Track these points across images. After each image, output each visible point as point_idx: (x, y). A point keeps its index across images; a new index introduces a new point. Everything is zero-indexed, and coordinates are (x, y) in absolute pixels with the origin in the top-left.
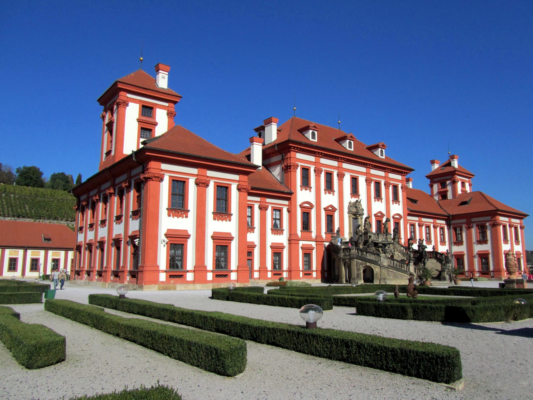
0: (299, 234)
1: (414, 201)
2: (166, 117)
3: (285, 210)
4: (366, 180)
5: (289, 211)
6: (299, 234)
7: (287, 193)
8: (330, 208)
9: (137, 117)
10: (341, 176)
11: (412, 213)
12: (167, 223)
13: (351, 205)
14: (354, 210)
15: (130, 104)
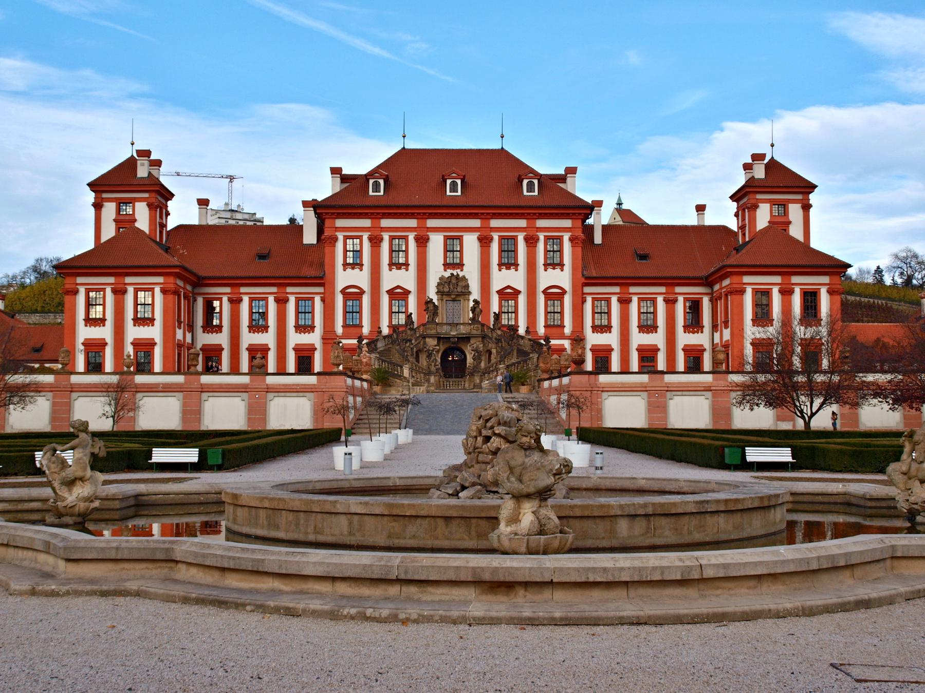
0: (339, 330)
1: (643, 257)
2: (147, 209)
3: (317, 299)
4: (480, 239)
5: (323, 300)
6: (339, 330)
7: (316, 278)
8: (399, 290)
9: (114, 216)
10: (422, 241)
11: (591, 281)
12: (84, 333)
13: (442, 282)
14: (446, 290)
15: (106, 204)
